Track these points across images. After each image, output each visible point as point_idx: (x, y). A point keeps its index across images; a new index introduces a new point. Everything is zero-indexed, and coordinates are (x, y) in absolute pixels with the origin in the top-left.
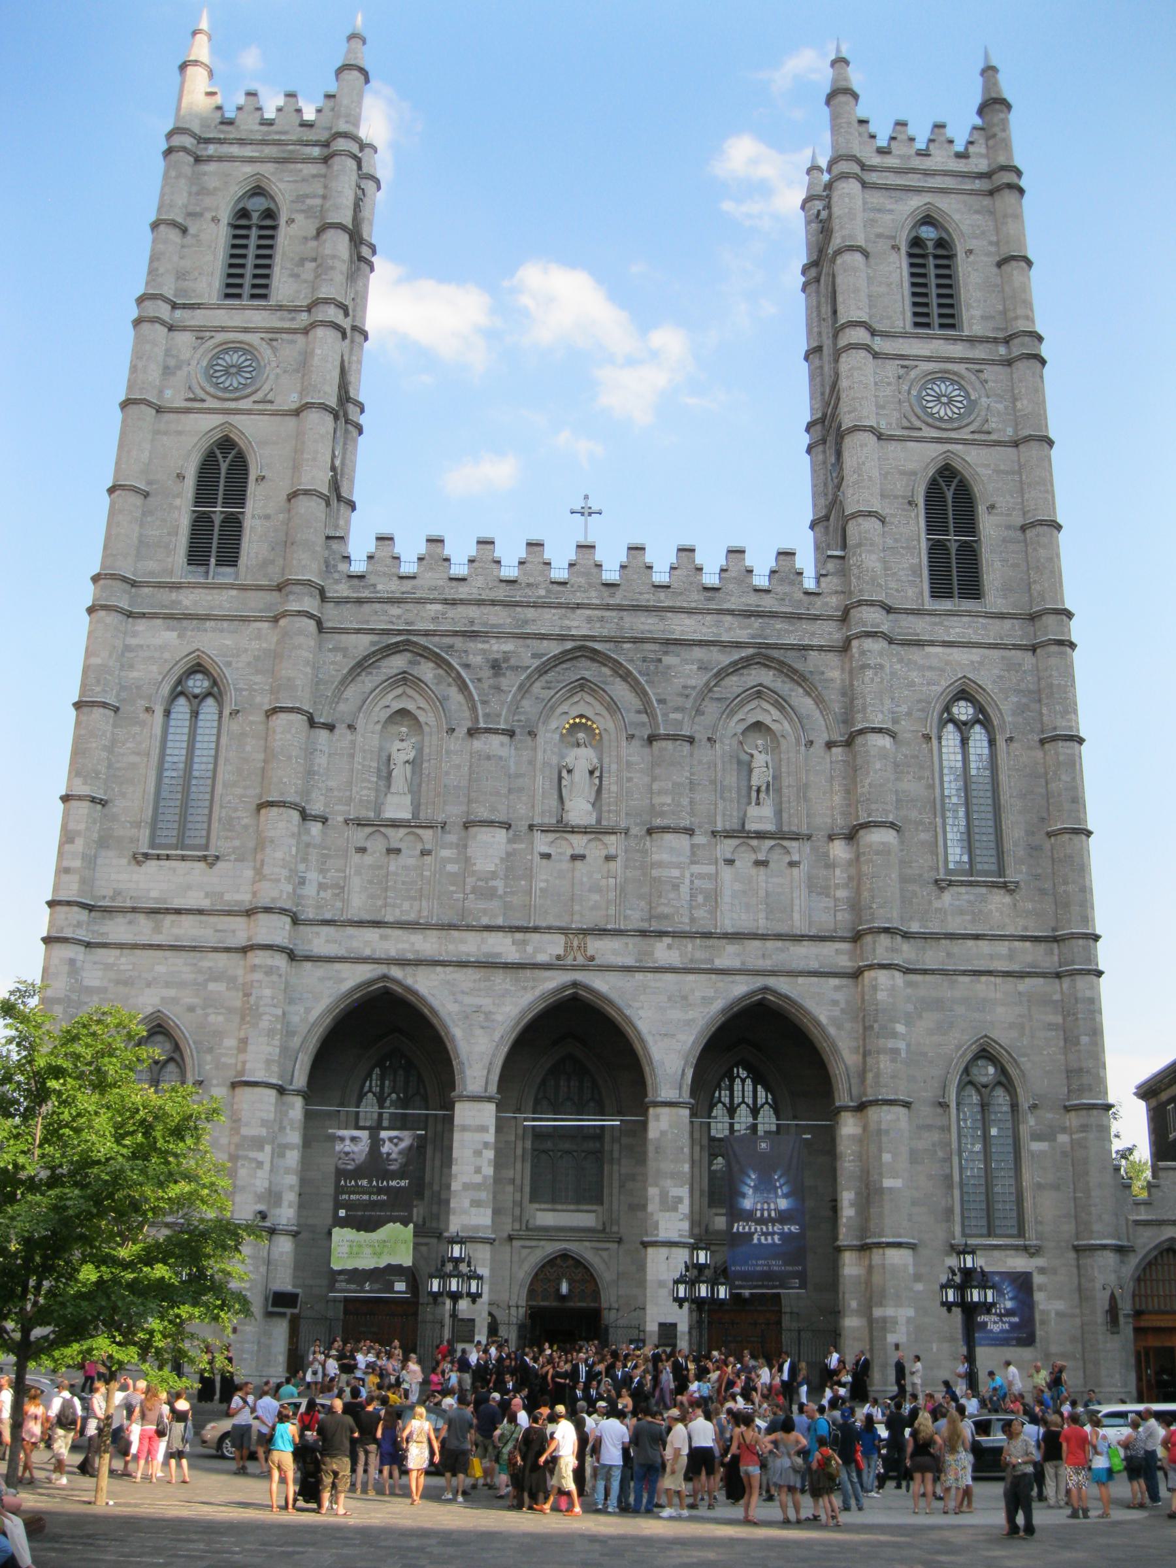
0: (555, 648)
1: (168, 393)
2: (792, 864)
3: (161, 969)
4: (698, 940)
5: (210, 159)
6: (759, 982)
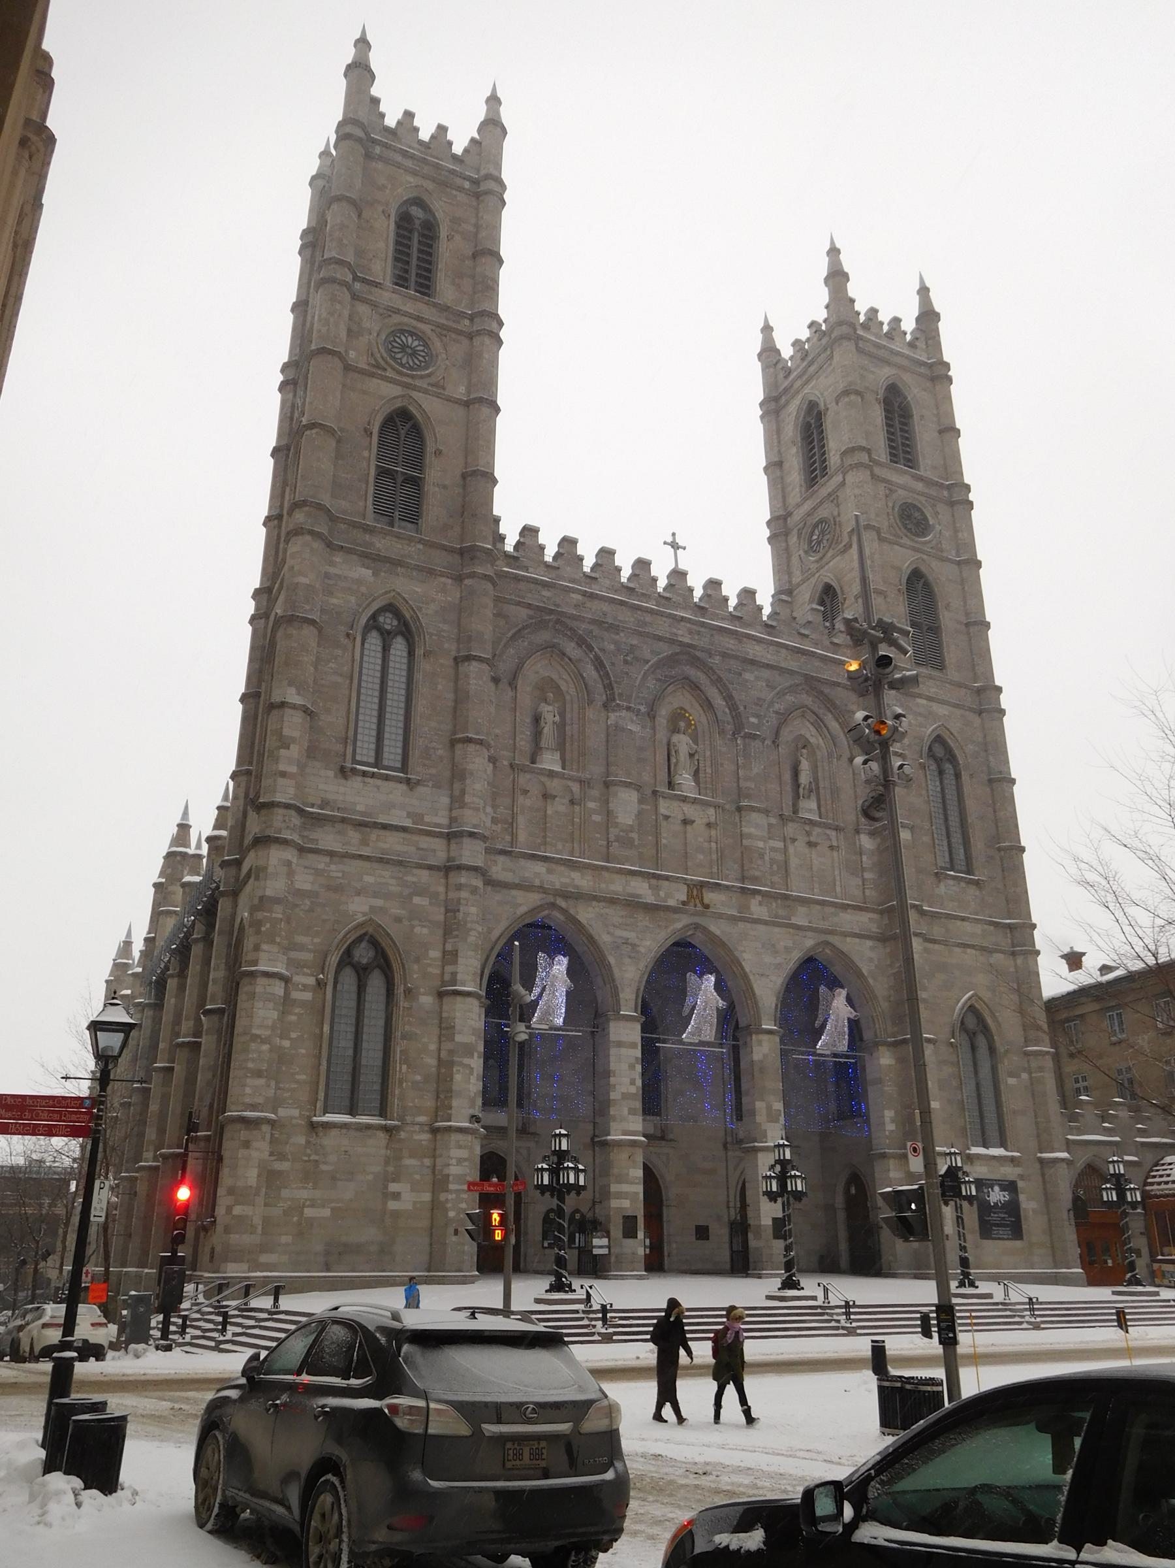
0: (666, 650)
2: (831, 847)
3: (369, 879)
5: (380, 158)
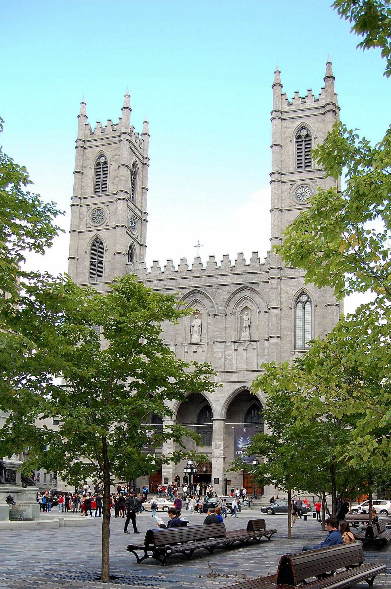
0: (187, 291)
1: (81, 226)
2: (254, 349)
5: (88, 147)
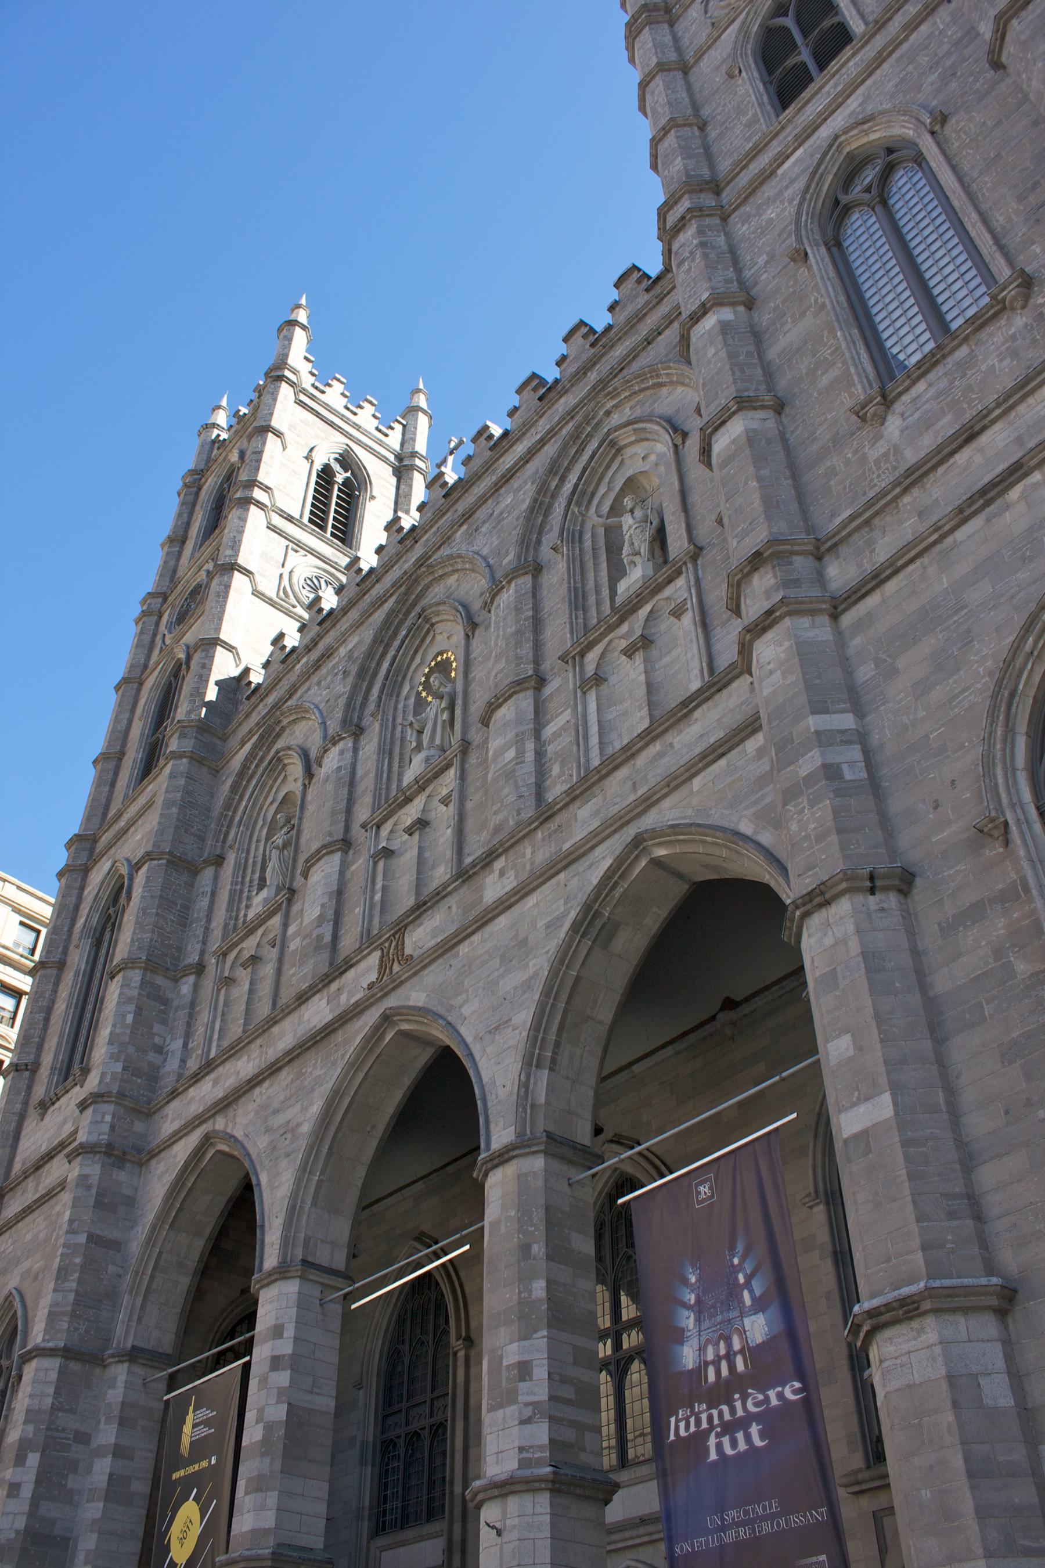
4: (539, 834)
6: (630, 832)
